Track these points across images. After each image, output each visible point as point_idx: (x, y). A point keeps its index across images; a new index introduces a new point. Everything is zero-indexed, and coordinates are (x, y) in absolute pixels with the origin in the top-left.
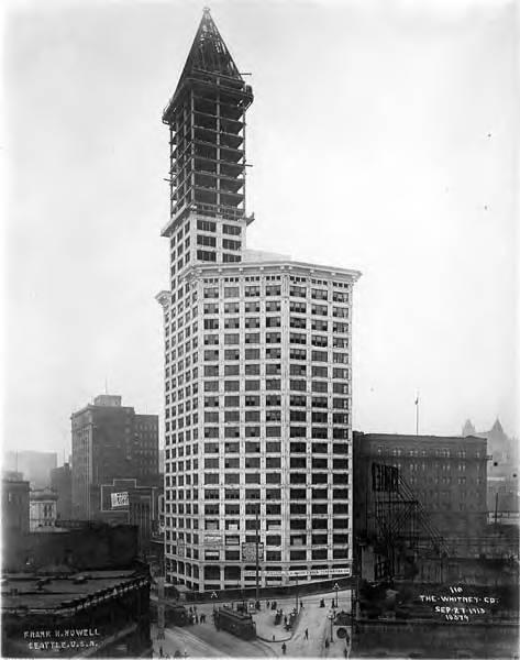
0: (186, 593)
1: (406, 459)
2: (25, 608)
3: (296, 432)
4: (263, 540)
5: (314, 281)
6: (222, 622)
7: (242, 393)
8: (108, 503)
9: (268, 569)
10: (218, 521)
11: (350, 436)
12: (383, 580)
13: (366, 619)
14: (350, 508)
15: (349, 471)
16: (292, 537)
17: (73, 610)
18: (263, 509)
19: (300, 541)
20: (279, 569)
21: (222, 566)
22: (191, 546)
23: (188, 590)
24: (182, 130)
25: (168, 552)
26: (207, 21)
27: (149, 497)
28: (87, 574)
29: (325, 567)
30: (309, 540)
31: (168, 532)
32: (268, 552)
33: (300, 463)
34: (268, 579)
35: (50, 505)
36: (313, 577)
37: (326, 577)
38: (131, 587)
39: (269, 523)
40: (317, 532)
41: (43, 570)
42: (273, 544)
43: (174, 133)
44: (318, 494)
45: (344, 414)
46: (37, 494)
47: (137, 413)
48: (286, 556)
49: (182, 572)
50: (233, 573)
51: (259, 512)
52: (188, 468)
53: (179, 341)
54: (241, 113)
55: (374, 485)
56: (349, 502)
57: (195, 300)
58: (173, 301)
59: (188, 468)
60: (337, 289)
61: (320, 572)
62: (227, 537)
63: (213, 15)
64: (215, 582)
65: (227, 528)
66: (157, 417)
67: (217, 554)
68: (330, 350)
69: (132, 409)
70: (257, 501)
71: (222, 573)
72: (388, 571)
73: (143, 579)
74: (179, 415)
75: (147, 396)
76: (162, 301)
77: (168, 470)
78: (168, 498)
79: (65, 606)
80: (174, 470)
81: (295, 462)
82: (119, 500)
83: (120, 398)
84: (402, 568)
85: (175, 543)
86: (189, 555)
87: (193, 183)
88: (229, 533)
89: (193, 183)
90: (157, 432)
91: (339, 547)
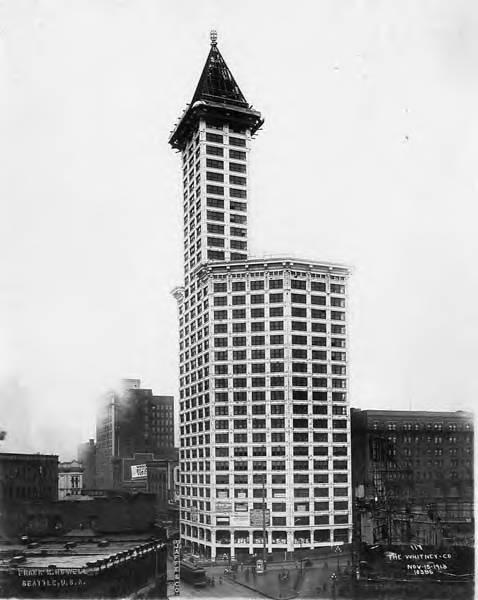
1: (401, 433)
2: (53, 567)
4: (269, 507)
5: (313, 275)
7: (249, 362)
8: (129, 473)
10: (228, 491)
11: (349, 413)
14: (349, 477)
16: (296, 505)
17: (97, 569)
18: (269, 479)
19: (304, 507)
22: (205, 512)
25: (183, 518)
27: (165, 469)
28: (110, 538)
30: (312, 507)
31: (183, 500)
35: (77, 476)
38: (150, 549)
39: (274, 491)
40: (318, 500)
41: (70, 534)
45: (341, 366)
46: (65, 466)
47: (154, 394)
52: (201, 443)
53: (192, 317)
55: (371, 457)
56: (348, 471)
58: (187, 295)
59: (201, 443)
65: (236, 496)
66: (172, 397)
67: (226, 520)
69: (150, 391)
70: (264, 472)
73: (160, 543)
74: (194, 391)
75: (165, 383)
76: (176, 294)
77: (182, 445)
78: (183, 469)
79: (90, 565)
80: (188, 444)
82: (137, 472)
83: (139, 381)
85: (189, 510)
86: (202, 521)
88: (239, 501)
90: (173, 419)
91: (339, 513)
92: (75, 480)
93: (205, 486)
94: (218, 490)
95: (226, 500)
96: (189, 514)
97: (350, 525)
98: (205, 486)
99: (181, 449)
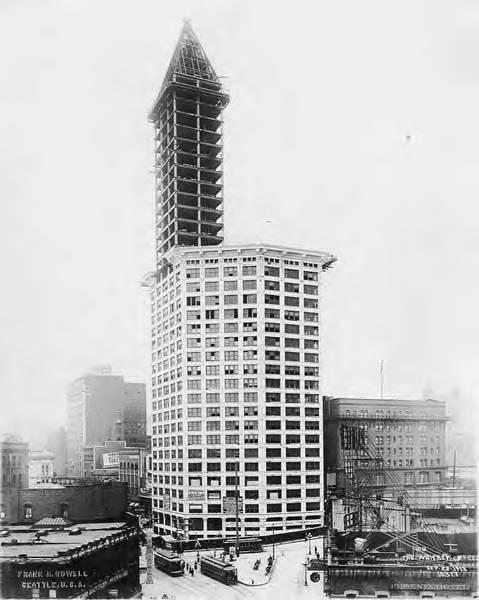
0: (173, 544)
1: (372, 421)
2: (24, 556)
3: (271, 425)
4: (242, 494)
5: (286, 262)
6: (208, 570)
8: (100, 465)
9: (247, 520)
10: (200, 478)
12: (352, 530)
13: (336, 564)
15: (320, 432)
16: (269, 492)
17: (69, 558)
18: (242, 467)
19: (276, 494)
20: (257, 520)
21: (205, 518)
22: (177, 500)
23: (173, 540)
24: (165, 127)
25: (156, 505)
26: (187, 30)
29: (299, 518)
30: (284, 494)
31: (156, 488)
32: (247, 506)
33: (276, 453)
34: (247, 529)
36: (288, 528)
37: (300, 527)
39: (247, 479)
41: (39, 523)
42: (251, 498)
43: (158, 130)
44: (291, 439)
48: (263, 508)
49: (168, 524)
50: (215, 524)
51: (238, 483)
54: (218, 112)
55: (343, 444)
56: (320, 459)
57: (178, 280)
60: (308, 269)
61: (294, 523)
62: (209, 492)
63: (194, 26)
64: (199, 533)
65: (209, 484)
67: (200, 507)
68: (302, 378)
71: (205, 524)
72: (356, 520)
73: (132, 530)
75: (137, 367)
77: (154, 433)
78: (155, 457)
79: (61, 554)
81: (270, 410)
84: (369, 519)
86: (174, 509)
87: (175, 175)
89: (175, 175)
92: (45, 468)
93: (177, 474)
94: (190, 478)
95: (200, 488)
96: (161, 501)
97: (321, 512)
98: (177, 474)
99: (153, 437)
